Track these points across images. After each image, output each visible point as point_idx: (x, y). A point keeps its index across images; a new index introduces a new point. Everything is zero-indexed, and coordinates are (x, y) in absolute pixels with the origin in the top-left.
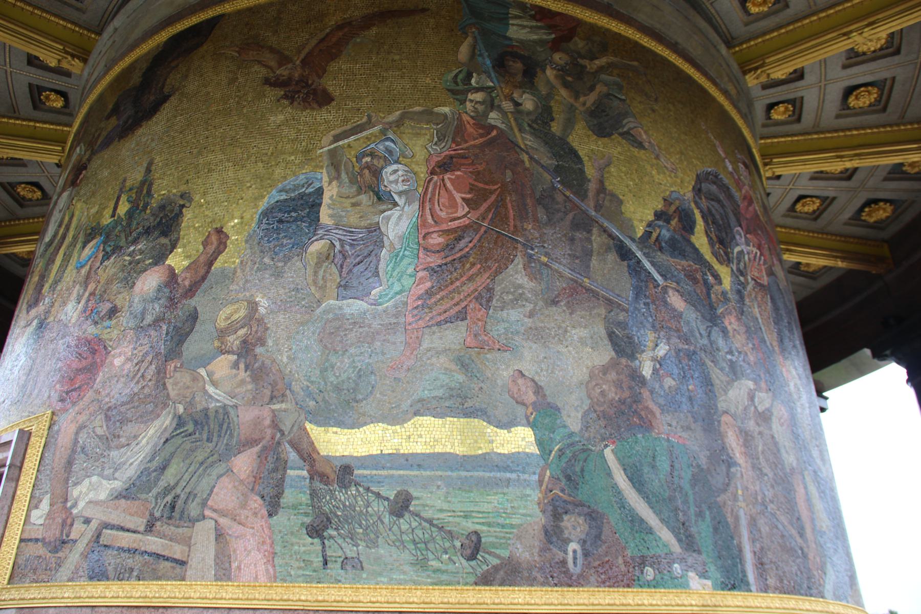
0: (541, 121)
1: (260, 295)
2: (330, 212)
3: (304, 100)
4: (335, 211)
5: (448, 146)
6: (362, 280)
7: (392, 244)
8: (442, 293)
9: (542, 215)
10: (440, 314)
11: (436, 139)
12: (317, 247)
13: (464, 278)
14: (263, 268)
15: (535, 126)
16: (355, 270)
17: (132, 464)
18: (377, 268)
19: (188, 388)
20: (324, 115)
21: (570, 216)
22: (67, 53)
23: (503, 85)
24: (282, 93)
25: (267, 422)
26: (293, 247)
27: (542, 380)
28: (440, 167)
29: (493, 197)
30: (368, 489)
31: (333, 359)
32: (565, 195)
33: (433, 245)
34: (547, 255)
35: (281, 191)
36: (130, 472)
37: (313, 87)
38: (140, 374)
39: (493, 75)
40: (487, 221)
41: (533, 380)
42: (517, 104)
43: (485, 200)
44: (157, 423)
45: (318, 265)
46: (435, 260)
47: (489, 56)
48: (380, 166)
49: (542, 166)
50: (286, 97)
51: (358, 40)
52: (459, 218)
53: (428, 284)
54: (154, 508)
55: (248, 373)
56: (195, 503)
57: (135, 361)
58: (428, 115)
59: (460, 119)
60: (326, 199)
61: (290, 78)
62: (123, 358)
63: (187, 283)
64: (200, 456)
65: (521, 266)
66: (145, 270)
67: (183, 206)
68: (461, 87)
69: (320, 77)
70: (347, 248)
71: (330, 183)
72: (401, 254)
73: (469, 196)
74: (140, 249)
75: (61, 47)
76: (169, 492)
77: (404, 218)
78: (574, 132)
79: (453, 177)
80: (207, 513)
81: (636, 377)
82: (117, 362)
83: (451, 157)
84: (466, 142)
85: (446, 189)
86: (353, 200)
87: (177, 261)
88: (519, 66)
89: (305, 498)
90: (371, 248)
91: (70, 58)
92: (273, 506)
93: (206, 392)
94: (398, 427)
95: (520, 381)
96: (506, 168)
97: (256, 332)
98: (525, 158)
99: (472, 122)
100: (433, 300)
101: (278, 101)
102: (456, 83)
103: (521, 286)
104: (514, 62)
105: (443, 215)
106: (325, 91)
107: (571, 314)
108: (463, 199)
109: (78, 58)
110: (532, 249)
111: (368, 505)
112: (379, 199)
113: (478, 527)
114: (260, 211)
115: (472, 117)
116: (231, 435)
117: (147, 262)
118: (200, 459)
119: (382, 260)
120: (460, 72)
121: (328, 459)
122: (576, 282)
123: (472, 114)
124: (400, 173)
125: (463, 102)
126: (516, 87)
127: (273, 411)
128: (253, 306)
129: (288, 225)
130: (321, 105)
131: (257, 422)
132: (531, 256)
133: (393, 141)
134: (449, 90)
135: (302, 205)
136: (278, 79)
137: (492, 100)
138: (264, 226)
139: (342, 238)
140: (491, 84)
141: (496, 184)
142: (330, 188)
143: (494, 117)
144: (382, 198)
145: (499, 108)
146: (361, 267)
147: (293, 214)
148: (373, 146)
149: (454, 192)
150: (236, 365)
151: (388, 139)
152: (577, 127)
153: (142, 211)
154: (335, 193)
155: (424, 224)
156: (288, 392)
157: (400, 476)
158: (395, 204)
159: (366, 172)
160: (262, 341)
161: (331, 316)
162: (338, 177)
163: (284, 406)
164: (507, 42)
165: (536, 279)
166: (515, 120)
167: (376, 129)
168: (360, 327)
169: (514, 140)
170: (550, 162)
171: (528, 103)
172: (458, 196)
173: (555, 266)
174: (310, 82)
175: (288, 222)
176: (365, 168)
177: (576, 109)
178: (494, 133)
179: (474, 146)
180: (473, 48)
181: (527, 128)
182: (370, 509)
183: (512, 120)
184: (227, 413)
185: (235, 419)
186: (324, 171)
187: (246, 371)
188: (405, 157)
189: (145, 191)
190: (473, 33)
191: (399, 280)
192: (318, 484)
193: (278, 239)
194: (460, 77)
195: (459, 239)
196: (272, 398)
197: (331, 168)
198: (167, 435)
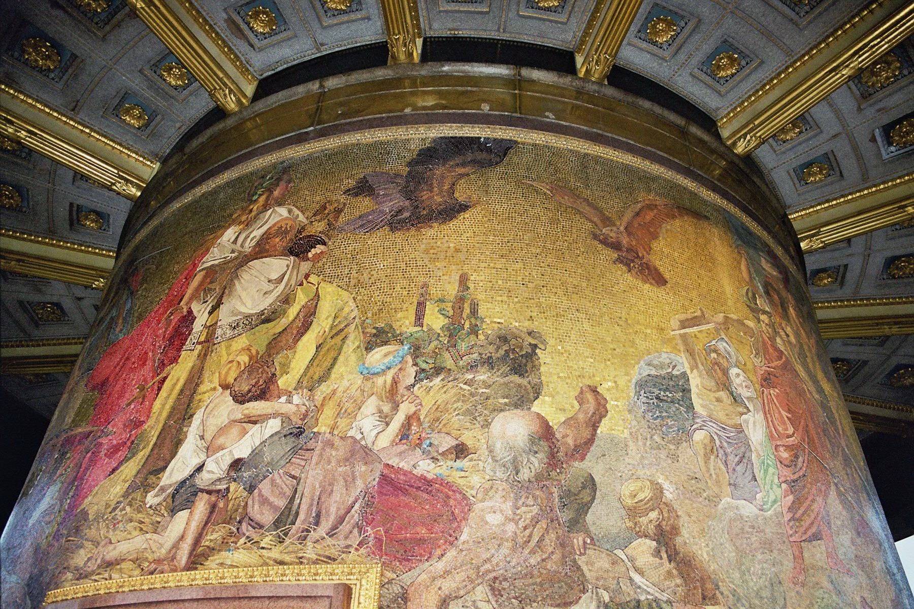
1: (661, 477)
7: (756, 450)
12: (699, 436)
26: (678, 430)
37: (644, 261)
50: (620, 260)
57: (521, 524)
70: (725, 444)
97: (669, 519)
114: (634, 381)
124: (741, 377)
128: (659, 490)
148: (714, 342)
150: (657, 553)
153: (469, 334)
156: (717, 592)
158: (749, 411)
159: (716, 367)
162: (697, 367)
187: (670, 561)
189: (467, 311)
193: (662, 418)
196: (704, 598)
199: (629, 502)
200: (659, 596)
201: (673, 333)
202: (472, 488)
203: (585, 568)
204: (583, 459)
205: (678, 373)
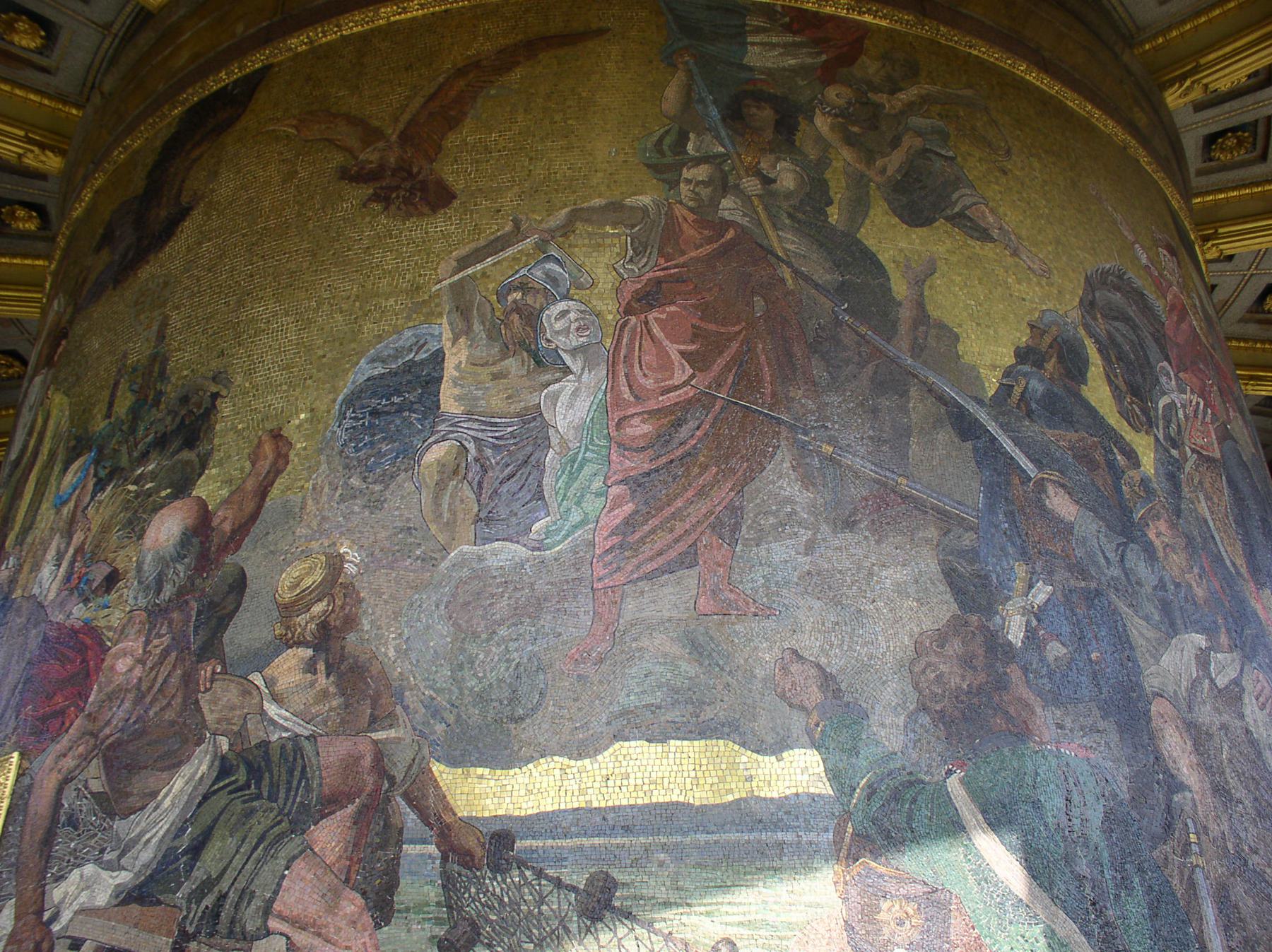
0: (809, 207)
2: (457, 391)
3: (407, 202)
4: (465, 391)
5: (652, 263)
6: (516, 506)
7: (563, 442)
8: (653, 523)
9: (818, 370)
10: (651, 559)
11: (631, 252)
12: (436, 453)
13: (690, 494)
14: (350, 495)
15: (800, 216)
16: (504, 489)
17: (148, 841)
18: (540, 486)
19: (233, 708)
20: (441, 225)
21: (870, 369)
22: (30, 141)
23: (741, 150)
24: (371, 191)
25: (367, 761)
27: (834, 664)
28: (639, 300)
29: (735, 346)
30: (540, 874)
31: (472, 648)
32: (858, 334)
33: (634, 438)
34: (831, 441)
35: (373, 361)
36: (146, 855)
37: (420, 177)
38: (158, 685)
39: (723, 134)
40: (725, 389)
41: (819, 666)
42: (767, 181)
43: (721, 353)
44: (186, 770)
45: (441, 486)
46: (638, 464)
47: (715, 102)
48: (538, 306)
49: (817, 286)
50: (376, 198)
51: (493, 92)
52: (676, 388)
53: (629, 508)
54: (185, 918)
55: (332, 678)
56: (253, 907)
58: (615, 211)
59: (670, 215)
60: (450, 370)
61: (382, 167)
62: (129, 661)
63: (227, 527)
64: (259, 825)
65: (786, 465)
66: (162, 507)
67: (215, 396)
68: (669, 159)
69: (432, 161)
70: (489, 452)
71: (455, 341)
72: (580, 456)
73: (692, 348)
74: (152, 472)
75: (22, 133)
76: (210, 890)
77: (583, 395)
78: (867, 221)
79: (664, 316)
80: (273, 924)
81: (996, 646)
82: (122, 665)
83: (659, 282)
84: (683, 253)
85: (653, 338)
86: (495, 369)
87: (209, 488)
88: (766, 114)
89: (433, 893)
90: (530, 449)
91: (36, 149)
92: (382, 906)
93: (263, 713)
94: (587, 762)
95: (794, 668)
96: (753, 293)
97: (342, 607)
98: (786, 273)
99: (691, 217)
100: (637, 536)
101: (364, 205)
102: (663, 154)
103: (789, 500)
104: (758, 108)
105: (649, 383)
106: (440, 184)
107: (878, 542)
108: (682, 353)
109: (52, 149)
110: (806, 434)
111: (542, 901)
112: (539, 363)
113: (731, 932)
114: (341, 398)
115: (691, 210)
116: (308, 789)
117: (163, 494)
118: (259, 829)
119: (548, 470)
120: (667, 132)
121: (469, 823)
122: (884, 485)
123: (691, 204)
124: (572, 315)
125: (674, 184)
126: (763, 151)
127: (376, 742)
128: (335, 564)
129: (389, 418)
130: (434, 209)
131: (351, 763)
132: (803, 445)
133: (558, 261)
134: (648, 166)
135: (410, 382)
136: (363, 168)
137: (724, 177)
138: (347, 423)
139: (480, 435)
140: (721, 149)
141: (738, 322)
142: (454, 350)
143: (728, 207)
144: (545, 362)
145: (738, 191)
146: (512, 485)
147: (396, 400)
148: (524, 272)
149: (666, 343)
150: (310, 667)
151: (549, 258)
152: (872, 213)
153: (152, 406)
154: (463, 359)
155: (618, 402)
156: (399, 709)
157: (593, 847)
158: (567, 371)
159: (515, 317)
160: (350, 622)
161: (465, 573)
162: (468, 331)
163: (392, 733)
164: (744, 75)
165: (814, 485)
166: (766, 208)
167: (529, 242)
168: (516, 589)
169: (765, 243)
170: (828, 277)
171: (787, 177)
172: (673, 350)
173: (847, 459)
174: (415, 170)
175: (387, 413)
176: (513, 310)
177: (870, 180)
178: (730, 234)
179: (698, 259)
180: (688, 89)
181: (787, 221)
182: (544, 907)
183: (760, 209)
184: (298, 749)
185: (314, 761)
186: (445, 320)
187: (328, 676)
188: (580, 287)
190: (686, 63)
191: (578, 504)
192: (456, 867)
194: (668, 141)
195: (678, 424)
197: (455, 315)
198: (203, 789)
199: (288, 596)
200: (299, 730)
201: (438, 287)
202: (110, 628)
203: (206, 710)
204: (238, 548)
205: (425, 356)
